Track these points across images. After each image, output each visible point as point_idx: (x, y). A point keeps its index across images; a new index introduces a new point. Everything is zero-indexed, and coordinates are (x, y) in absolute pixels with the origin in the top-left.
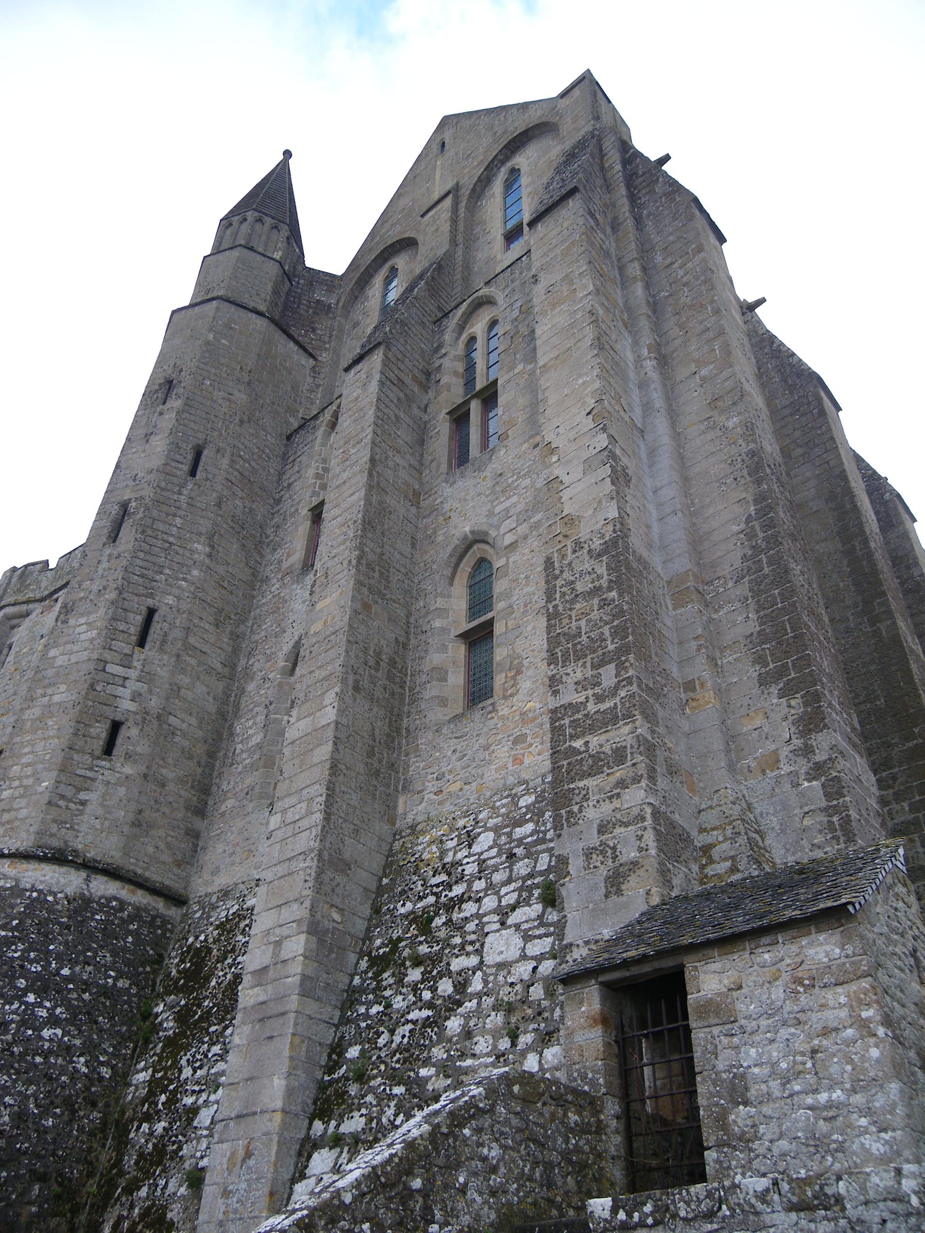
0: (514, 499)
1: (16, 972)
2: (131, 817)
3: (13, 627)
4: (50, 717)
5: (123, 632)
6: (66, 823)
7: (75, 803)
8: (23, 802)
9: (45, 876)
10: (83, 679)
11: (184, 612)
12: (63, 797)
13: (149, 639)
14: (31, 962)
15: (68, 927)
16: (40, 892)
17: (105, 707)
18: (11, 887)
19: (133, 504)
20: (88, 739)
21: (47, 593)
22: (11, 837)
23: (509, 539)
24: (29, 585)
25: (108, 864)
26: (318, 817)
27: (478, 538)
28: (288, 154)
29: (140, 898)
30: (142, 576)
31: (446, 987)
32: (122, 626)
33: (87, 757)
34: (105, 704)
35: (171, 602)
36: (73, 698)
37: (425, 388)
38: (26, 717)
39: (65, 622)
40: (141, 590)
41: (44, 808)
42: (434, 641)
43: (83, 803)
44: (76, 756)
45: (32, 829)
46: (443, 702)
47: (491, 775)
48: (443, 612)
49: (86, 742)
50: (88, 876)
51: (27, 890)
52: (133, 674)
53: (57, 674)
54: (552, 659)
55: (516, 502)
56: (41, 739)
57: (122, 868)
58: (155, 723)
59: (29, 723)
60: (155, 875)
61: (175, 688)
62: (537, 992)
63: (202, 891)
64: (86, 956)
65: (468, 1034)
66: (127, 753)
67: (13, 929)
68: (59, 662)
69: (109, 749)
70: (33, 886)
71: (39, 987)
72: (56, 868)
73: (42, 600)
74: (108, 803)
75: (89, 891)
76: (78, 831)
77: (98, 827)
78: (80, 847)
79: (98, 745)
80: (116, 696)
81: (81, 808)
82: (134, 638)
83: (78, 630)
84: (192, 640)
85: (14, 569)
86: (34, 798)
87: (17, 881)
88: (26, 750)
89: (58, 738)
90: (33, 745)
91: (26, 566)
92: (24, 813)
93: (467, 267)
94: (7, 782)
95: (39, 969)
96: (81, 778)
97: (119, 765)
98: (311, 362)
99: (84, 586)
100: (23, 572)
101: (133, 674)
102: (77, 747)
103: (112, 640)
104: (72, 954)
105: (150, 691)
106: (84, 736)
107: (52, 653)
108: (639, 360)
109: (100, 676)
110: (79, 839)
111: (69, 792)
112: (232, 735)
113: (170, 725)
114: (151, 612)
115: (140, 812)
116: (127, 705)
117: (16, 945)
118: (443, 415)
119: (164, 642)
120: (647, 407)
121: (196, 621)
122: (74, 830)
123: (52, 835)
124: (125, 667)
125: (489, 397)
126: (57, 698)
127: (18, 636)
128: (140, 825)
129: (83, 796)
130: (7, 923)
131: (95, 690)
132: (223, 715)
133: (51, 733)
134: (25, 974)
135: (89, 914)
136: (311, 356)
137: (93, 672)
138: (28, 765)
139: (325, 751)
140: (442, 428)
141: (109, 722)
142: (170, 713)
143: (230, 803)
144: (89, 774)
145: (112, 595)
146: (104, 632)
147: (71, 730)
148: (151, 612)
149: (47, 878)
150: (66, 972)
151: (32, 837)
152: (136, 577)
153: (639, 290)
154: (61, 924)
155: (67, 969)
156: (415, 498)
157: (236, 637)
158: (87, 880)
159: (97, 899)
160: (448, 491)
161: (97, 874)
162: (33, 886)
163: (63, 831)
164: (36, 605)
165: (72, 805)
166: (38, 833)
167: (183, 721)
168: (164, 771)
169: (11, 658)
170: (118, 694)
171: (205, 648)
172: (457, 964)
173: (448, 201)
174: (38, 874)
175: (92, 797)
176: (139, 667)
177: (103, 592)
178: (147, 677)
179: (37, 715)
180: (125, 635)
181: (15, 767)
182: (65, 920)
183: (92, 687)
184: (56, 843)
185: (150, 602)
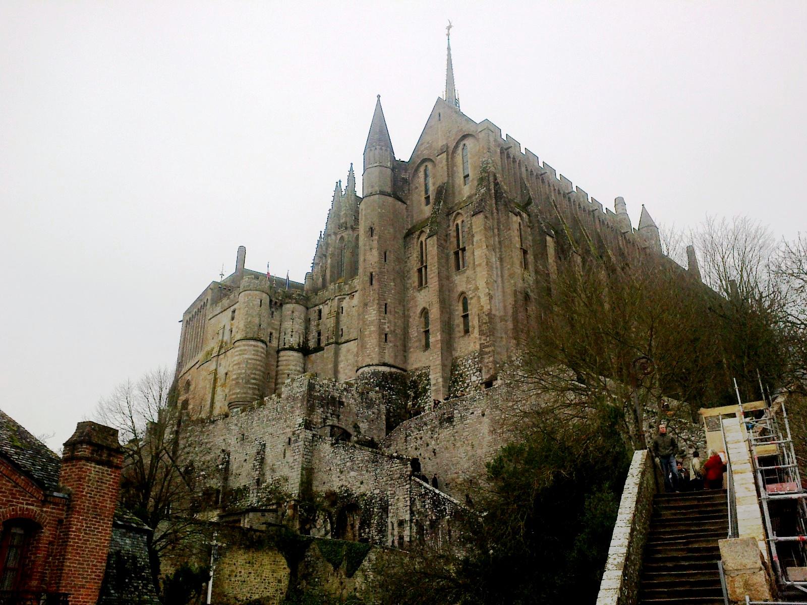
0: (471, 286)
19: (373, 273)
23: (471, 296)
26: (440, 358)
27: (463, 293)
28: (379, 96)
29: (399, 371)
31: (466, 385)
37: (446, 241)
42: (456, 318)
46: (460, 332)
47: (470, 349)
48: (457, 310)
54: (479, 335)
55: (472, 286)
60: (400, 366)
62: (479, 385)
63: (410, 369)
65: (470, 391)
68: (369, 319)
93: (453, 187)
98: (405, 205)
108: (496, 260)
112: (408, 333)
116: (387, 330)
118: (452, 252)
120: (497, 275)
125: (464, 250)
126: (372, 329)
132: (405, 327)
136: (405, 203)
139: (439, 345)
140: (452, 257)
143: (412, 350)
145: (377, 302)
148: (386, 304)
153: (497, 239)
156: (448, 278)
157: (404, 306)
160: (456, 278)
171: (398, 311)
172: (467, 381)
173: (444, 155)
175: (386, 351)
178: (389, 322)
185: (385, 302)
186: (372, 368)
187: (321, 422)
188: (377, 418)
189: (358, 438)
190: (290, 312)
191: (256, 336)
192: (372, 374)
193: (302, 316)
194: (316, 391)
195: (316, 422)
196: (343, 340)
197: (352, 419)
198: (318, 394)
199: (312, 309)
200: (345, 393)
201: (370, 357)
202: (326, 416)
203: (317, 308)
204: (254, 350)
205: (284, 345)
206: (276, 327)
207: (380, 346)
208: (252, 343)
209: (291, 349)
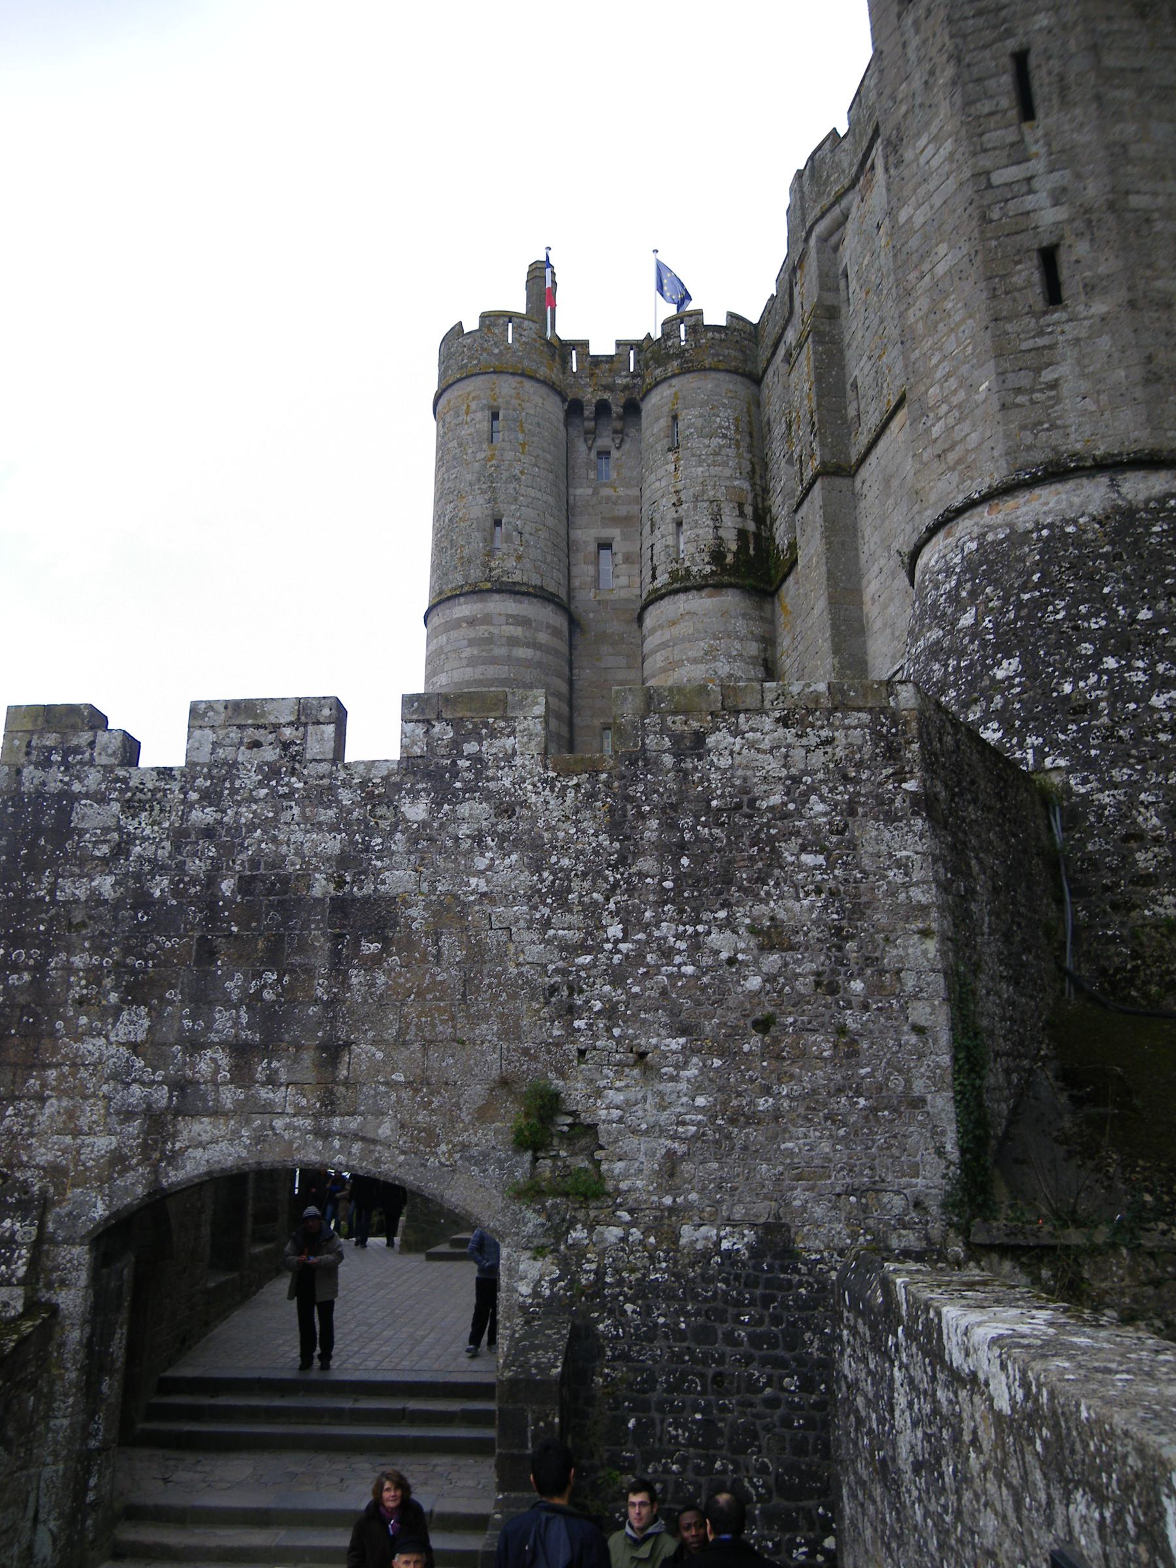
1: (1070, 637)
2: (1138, 372)
3: (836, 249)
4: (945, 298)
5: (991, 114)
6: (1041, 423)
7: (1041, 391)
8: (966, 427)
9: (1047, 504)
10: (966, 215)
11: (1075, 24)
12: (1018, 391)
13: (1037, 101)
14: (1087, 618)
15: (1118, 556)
16: (1050, 526)
17: (1019, 237)
18: (1007, 538)
20: (1016, 294)
21: (855, 168)
22: (972, 479)
24: (828, 177)
25: (1135, 452)
30: (979, 13)
32: (986, 107)
33: (1027, 319)
34: (1017, 233)
35: (1045, 23)
36: (965, 251)
38: (912, 320)
39: (899, 163)
40: (988, 35)
41: (999, 417)
43: (1054, 385)
44: (1009, 327)
45: (996, 453)
49: (1014, 300)
50: (1112, 480)
51: (1031, 532)
52: (1037, 166)
53: (926, 238)
56: (948, 335)
57: (1161, 451)
58: (1110, 219)
59: (920, 325)
61: (1116, 149)
64: (1165, 587)
66: (1085, 286)
67: (1037, 587)
68: (919, 220)
69: (1054, 295)
70: (1037, 523)
71: (1114, 645)
72: (1058, 487)
73: (852, 186)
74: (1091, 369)
75: (1124, 499)
76: (1065, 427)
77: (1093, 408)
78: (1078, 446)
79: (1035, 295)
80: (1028, 213)
81: (1053, 393)
82: (1013, 114)
83: (922, 160)
84: (1111, 60)
85: (799, 174)
86: (978, 412)
87: (1011, 526)
88: (934, 361)
89: (971, 316)
90: (940, 349)
91: (811, 158)
92: (974, 437)
94: (931, 415)
95: (1103, 623)
96: (1033, 354)
97: (1081, 308)
99: (900, 96)
100: (813, 168)
101: (1037, 166)
102: (1005, 313)
103: (981, 135)
104: (1142, 589)
105: (1078, 176)
106: (1007, 293)
107: (903, 217)
109: (989, 197)
110: (1072, 436)
111: (1024, 380)
113: (1136, 211)
114: (1021, 59)
115: (1150, 359)
117: (1052, 604)
119: (1063, 91)
121: (1103, 26)
122: (1058, 427)
123: (1029, 448)
124: (1019, 163)
126: (940, 269)
127: (848, 253)
128: (1159, 379)
129: (1047, 376)
130: (1025, 583)
131: (991, 221)
133: (957, 318)
134: (1086, 635)
135: (1140, 530)
137: (976, 197)
138: (947, 377)
141: (1035, 255)
142: (1127, 193)
144: (1040, 342)
146: (963, 132)
147: (984, 295)
148: (1021, 59)
149: (1051, 505)
150: (1144, 614)
151: (1002, 463)
152: (971, 22)
154: (1104, 556)
155: (1145, 611)
158: (1114, 486)
159: (1141, 506)
161: (1123, 472)
162: (1037, 523)
163: (1043, 436)
164: (850, 196)
165: (1037, 396)
166: (1007, 454)
167: (1155, 194)
168: (1159, 284)
169: (854, 285)
170: (1030, 208)
174: (1035, 505)
175: (1064, 370)
176: (1043, 151)
177: (931, 81)
178: (1062, 158)
179: (925, 308)
180: (998, 117)
181: (931, 390)
182: (1107, 549)
183: (984, 219)
184: (1040, 456)
185: (1011, 44)
186: (965, 526)
187: (117, 1160)
188: (827, 984)
189: (570, 1262)
190: (664, 422)
191: (475, 573)
192: (970, 566)
193: (724, 418)
194: (84, 864)
195: (55, 1171)
196: (864, 439)
197: (492, 1064)
198: (105, 884)
199: (770, 372)
200: (416, 811)
201: (952, 457)
202: (181, 1085)
203: (781, 351)
204: (471, 643)
205: (654, 578)
206: (622, 510)
207: (1001, 351)
208: (463, 609)
209: (683, 584)
